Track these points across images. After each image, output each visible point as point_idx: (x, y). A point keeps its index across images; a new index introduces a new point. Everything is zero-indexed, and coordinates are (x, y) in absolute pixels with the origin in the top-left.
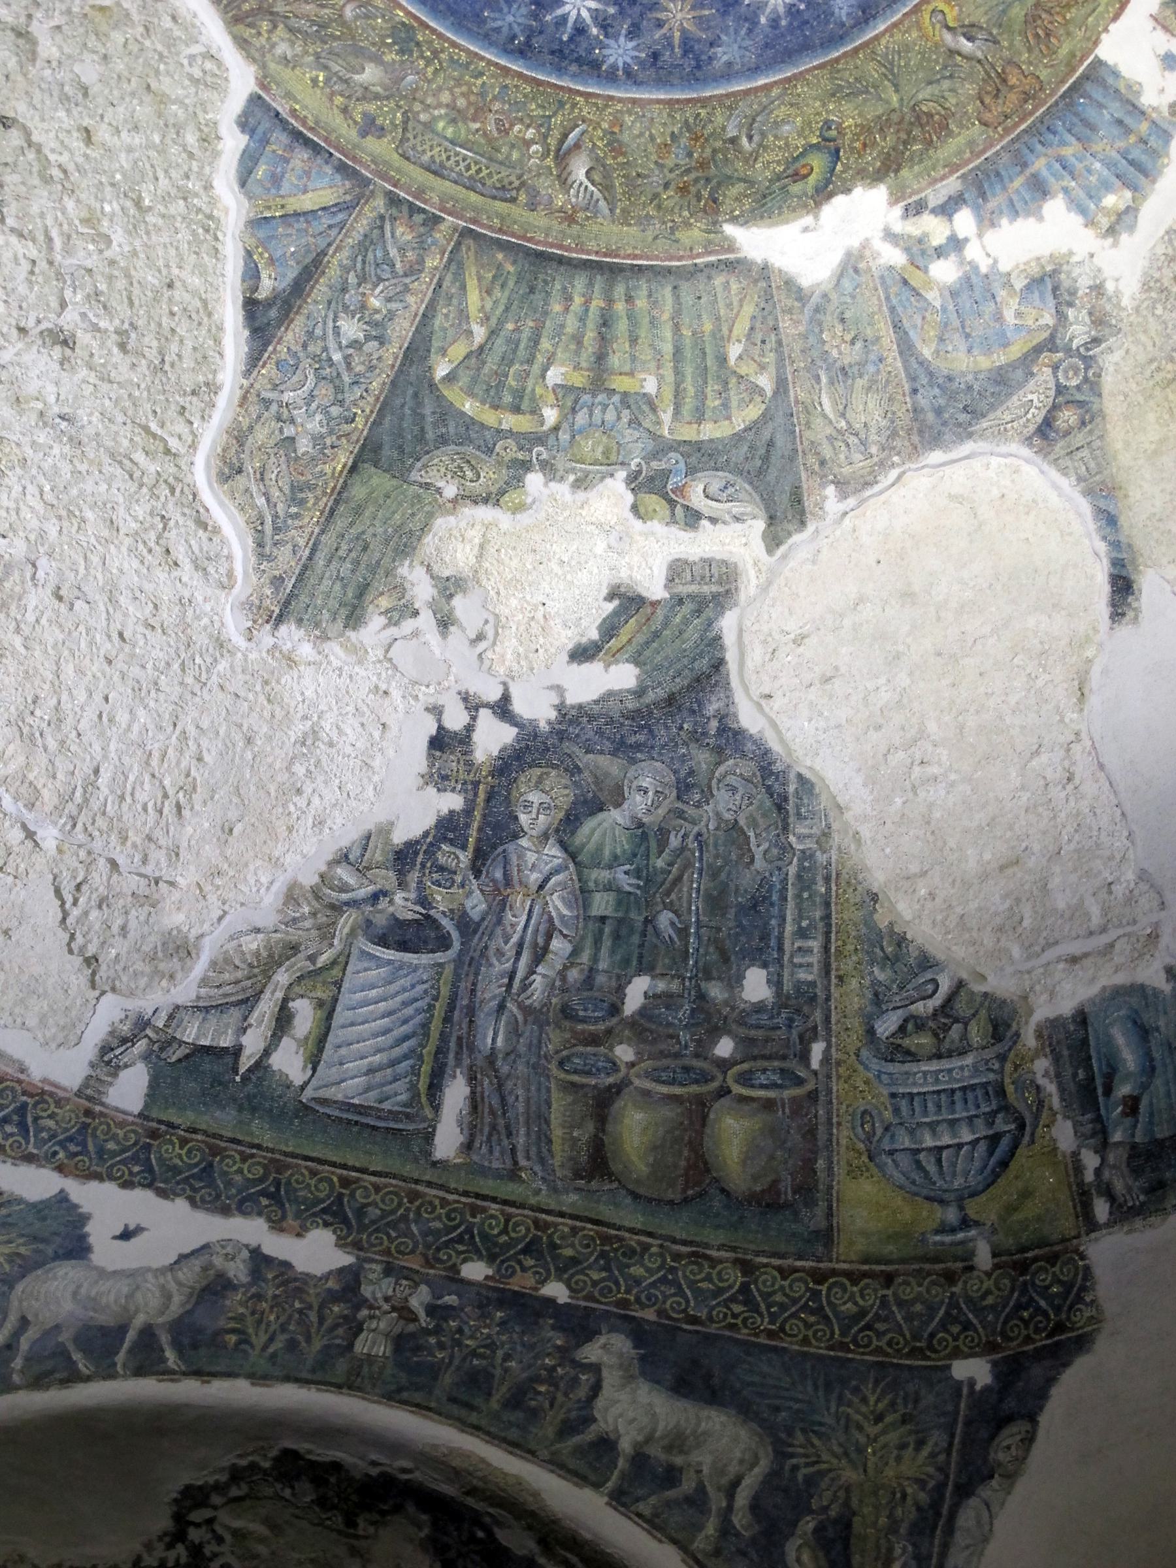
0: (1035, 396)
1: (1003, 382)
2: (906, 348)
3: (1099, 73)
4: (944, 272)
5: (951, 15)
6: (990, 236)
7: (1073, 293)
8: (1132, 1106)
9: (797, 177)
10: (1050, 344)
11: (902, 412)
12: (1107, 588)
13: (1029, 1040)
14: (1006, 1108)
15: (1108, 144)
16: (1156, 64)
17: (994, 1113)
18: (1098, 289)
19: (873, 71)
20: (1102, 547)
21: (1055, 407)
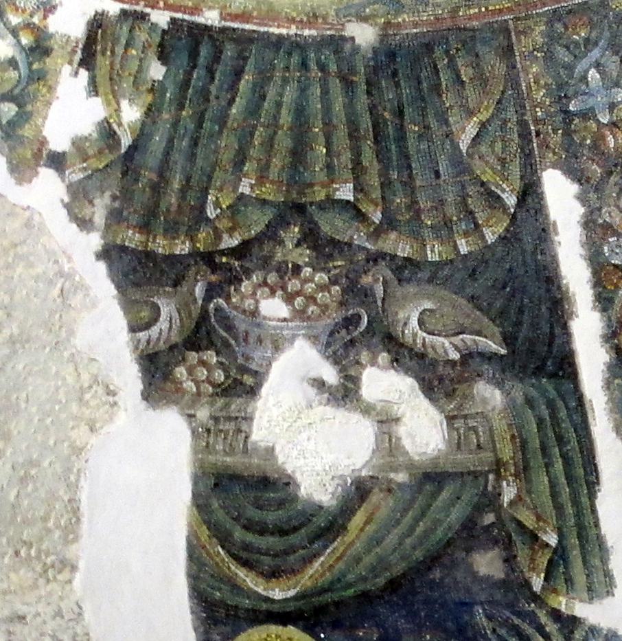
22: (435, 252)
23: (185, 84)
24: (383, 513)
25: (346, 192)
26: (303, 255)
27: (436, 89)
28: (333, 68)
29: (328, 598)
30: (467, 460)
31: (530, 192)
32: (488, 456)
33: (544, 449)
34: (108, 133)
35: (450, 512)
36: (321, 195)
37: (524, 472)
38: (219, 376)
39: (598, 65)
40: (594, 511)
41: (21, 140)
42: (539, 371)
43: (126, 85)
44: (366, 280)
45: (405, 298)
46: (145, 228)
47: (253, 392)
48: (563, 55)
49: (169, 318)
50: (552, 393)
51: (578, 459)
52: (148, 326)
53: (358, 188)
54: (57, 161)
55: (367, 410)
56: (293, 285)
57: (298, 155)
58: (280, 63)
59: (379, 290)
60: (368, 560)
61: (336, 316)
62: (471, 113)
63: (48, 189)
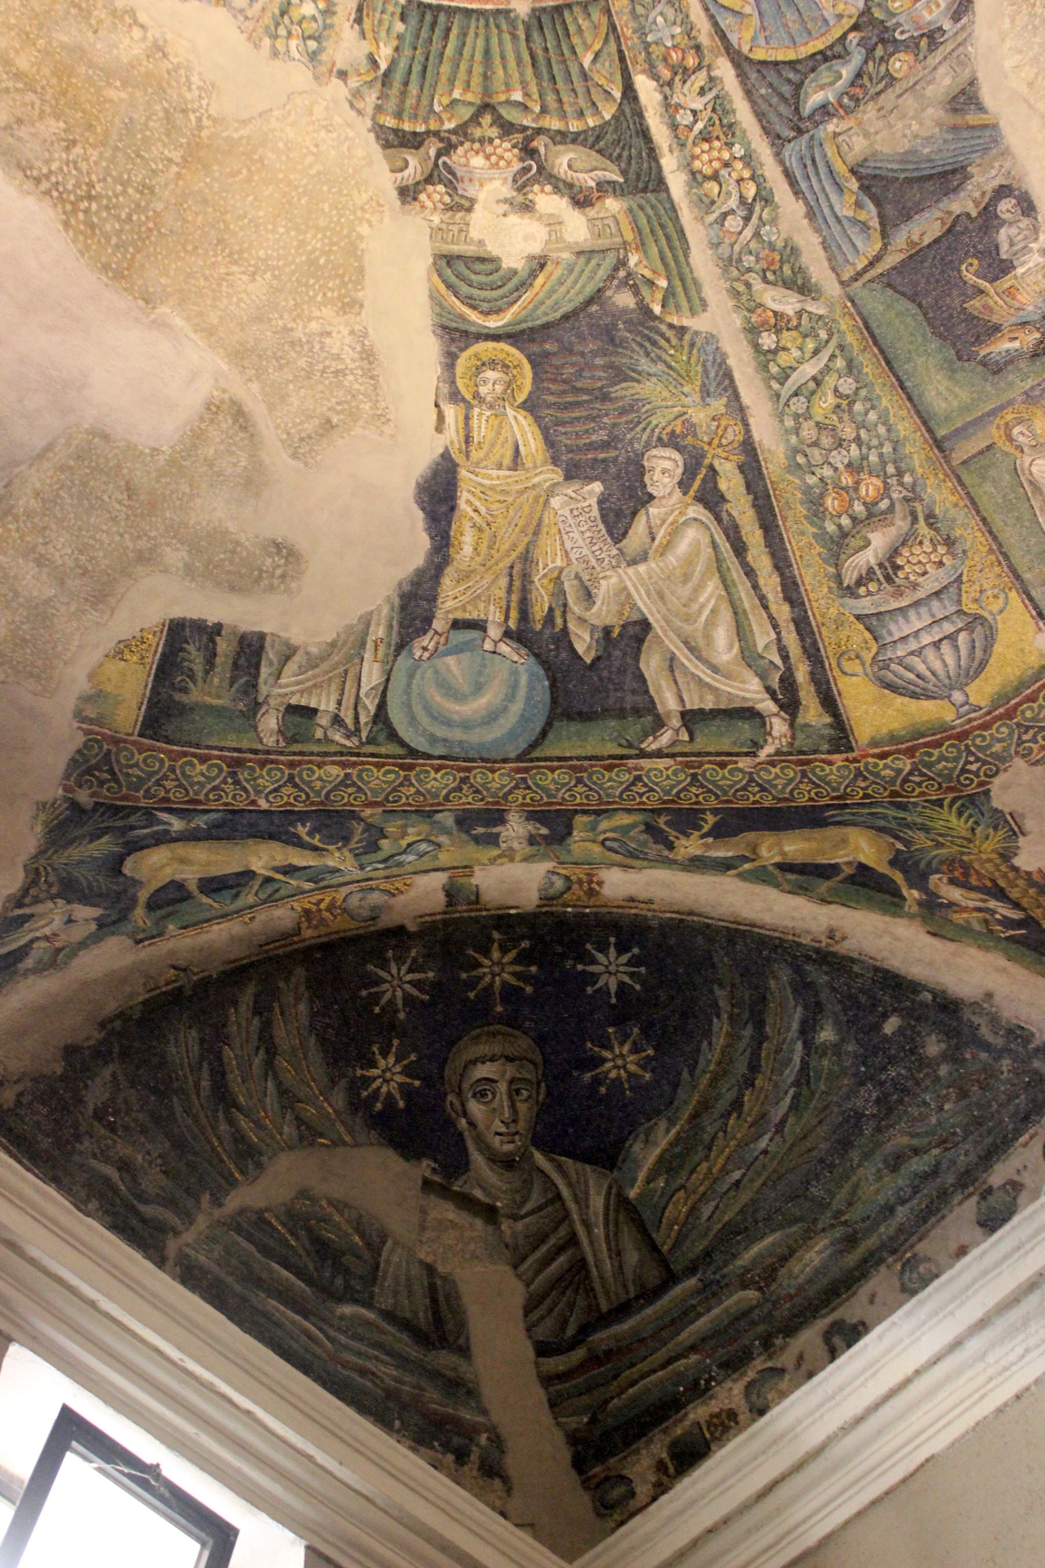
22: (575, 126)
23: (417, 37)
24: (554, 277)
25: (517, 96)
26: (494, 132)
27: (568, 36)
28: (504, 27)
29: (524, 326)
31: (629, 91)
32: (619, 240)
33: (652, 231)
36: (502, 98)
37: (642, 246)
38: (447, 199)
39: (661, 14)
40: (688, 264)
41: (320, 62)
42: (645, 190)
43: (383, 34)
44: (535, 144)
45: (558, 154)
46: (399, 115)
47: (469, 210)
48: (640, 10)
49: (415, 166)
50: (654, 201)
51: (675, 236)
52: (401, 170)
53: (527, 95)
54: (343, 75)
55: (540, 219)
56: (489, 149)
58: (473, 25)
59: (542, 150)
60: (549, 302)
61: (517, 166)
62: (587, 47)
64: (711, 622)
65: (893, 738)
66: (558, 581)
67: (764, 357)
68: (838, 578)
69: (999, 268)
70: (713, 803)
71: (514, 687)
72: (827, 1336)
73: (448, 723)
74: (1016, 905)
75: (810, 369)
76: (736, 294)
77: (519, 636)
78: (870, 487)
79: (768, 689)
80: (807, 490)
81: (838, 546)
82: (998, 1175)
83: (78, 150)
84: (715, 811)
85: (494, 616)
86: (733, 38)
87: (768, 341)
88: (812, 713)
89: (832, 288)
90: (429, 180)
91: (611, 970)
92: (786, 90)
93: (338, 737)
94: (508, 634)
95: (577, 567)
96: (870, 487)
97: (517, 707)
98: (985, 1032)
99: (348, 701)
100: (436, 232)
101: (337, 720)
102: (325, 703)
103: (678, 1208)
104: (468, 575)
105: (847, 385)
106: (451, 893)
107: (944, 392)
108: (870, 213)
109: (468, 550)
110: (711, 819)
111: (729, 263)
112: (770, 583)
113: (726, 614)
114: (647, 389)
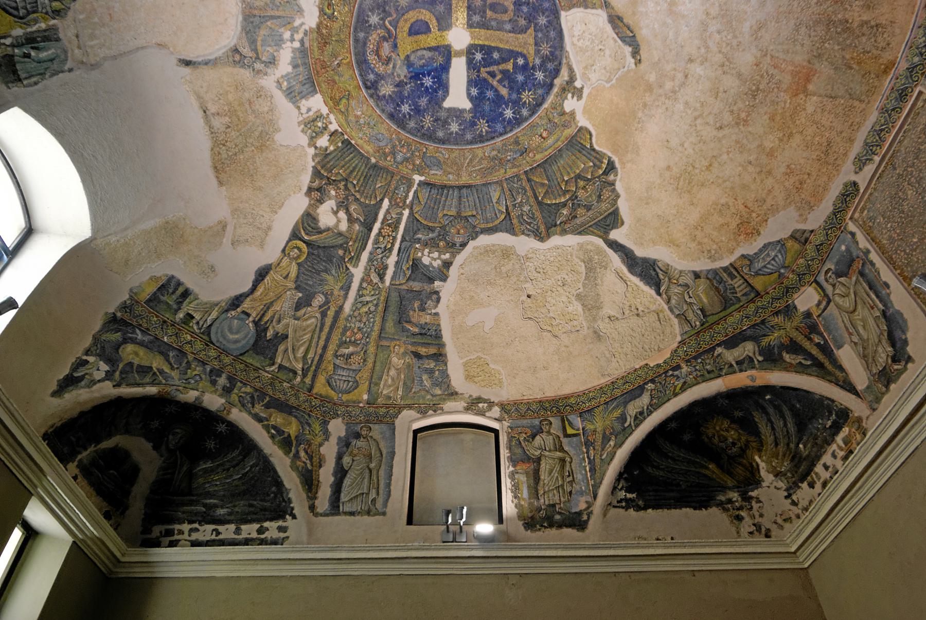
0: (246, 51)
1: (253, 42)
2: (272, 17)
3: (314, 92)
4: (287, 35)
5: (344, 61)
6: (290, 50)
7: (268, 67)
8: (27, 56)
9: (329, 5)
10: (258, 58)
11: (256, 12)
12: (188, 59)
13: (52, 22)
14: (29, 13)
15: (297, 88)
16: (310, 106)
17: (26, 9)
18: (266, 74)
19: (342, 37)
20: (200, 60)
21: (241, 55)
22: (362, 200)
25: (355, 182)
26: (342, 187)
30: (347, 234)
31: (382, 200)
34: (326, 149)
35: (340, 241)
49: (316, 184)
54: (316, 148)
57: (352, 172)
63: (312, 151)
64: (302, 345)
65: (321, 396)
66: (275, 314)
67: (361, 288)
68: (337, 351)
69: (422, 309)
70: (271, 393)
71: (246, 337)
72: (214, 530)
73: (225, 338)
74: (312, 465)
75: (368, 299)
76: (366, 269)
77: (256, 323)
78: (359, 336)
79: (303, 369)
80: (346, 326)
81: (342, 344)
82: (267, 524)
83: (229, 130)
84: (270, 397)
85: (254, 315)
86: (414, 207)
87: (365, 285)
88: (308, 380)
89: (387, 283)
90: (317, 190)
91: (222, 428)
92: (415, 228)
93: (195, 327)
94: (254, 321)
95: (282, 312)
96: (359, 336)
97: (243, 342)
98: (285, 495)
99: (204, 319)
100: (310, 205)
101: (198, 323)
102: (197, 316)
103: (201, 480)
104: (254, 300)
105: (372, 309)
106: (197, 399)
107: (390, 326)
108: (409, 273)
109: (259, 293)
110: (268, 399)
111: (370, 260)
112: (322, 343)
113: (307, 345)
114: (330, 278)
